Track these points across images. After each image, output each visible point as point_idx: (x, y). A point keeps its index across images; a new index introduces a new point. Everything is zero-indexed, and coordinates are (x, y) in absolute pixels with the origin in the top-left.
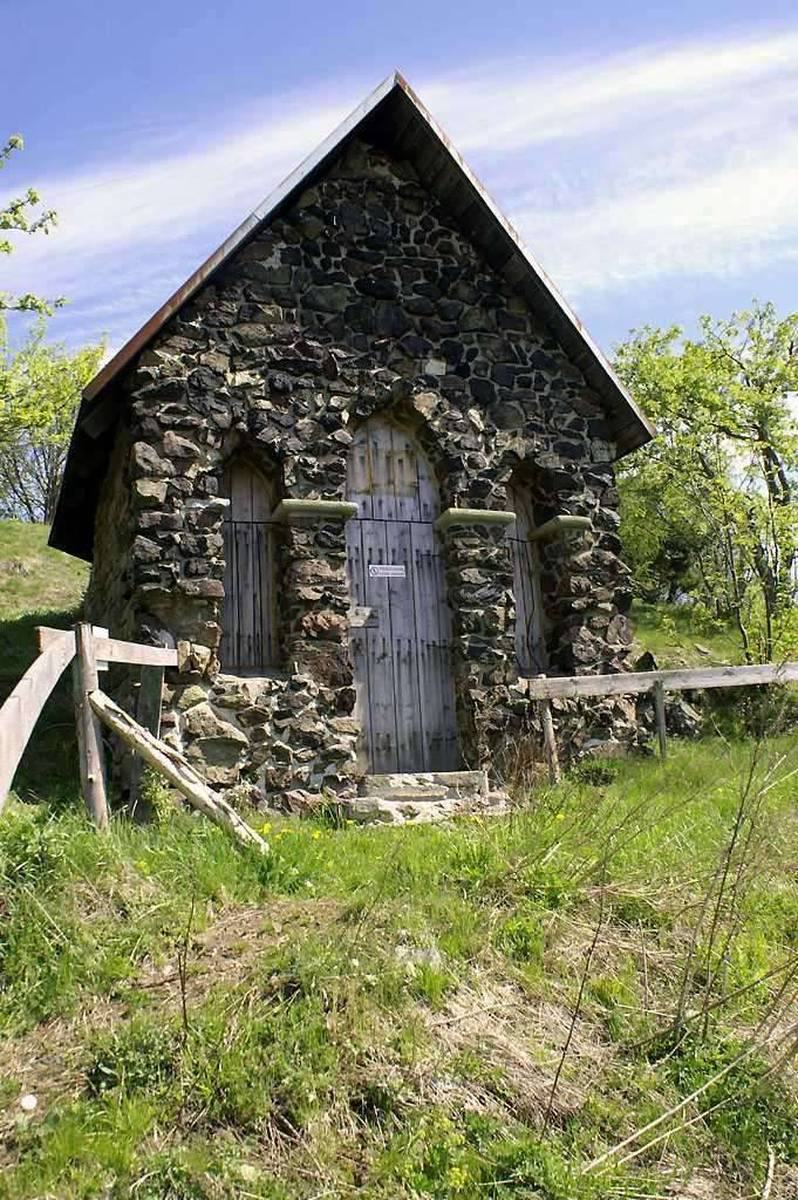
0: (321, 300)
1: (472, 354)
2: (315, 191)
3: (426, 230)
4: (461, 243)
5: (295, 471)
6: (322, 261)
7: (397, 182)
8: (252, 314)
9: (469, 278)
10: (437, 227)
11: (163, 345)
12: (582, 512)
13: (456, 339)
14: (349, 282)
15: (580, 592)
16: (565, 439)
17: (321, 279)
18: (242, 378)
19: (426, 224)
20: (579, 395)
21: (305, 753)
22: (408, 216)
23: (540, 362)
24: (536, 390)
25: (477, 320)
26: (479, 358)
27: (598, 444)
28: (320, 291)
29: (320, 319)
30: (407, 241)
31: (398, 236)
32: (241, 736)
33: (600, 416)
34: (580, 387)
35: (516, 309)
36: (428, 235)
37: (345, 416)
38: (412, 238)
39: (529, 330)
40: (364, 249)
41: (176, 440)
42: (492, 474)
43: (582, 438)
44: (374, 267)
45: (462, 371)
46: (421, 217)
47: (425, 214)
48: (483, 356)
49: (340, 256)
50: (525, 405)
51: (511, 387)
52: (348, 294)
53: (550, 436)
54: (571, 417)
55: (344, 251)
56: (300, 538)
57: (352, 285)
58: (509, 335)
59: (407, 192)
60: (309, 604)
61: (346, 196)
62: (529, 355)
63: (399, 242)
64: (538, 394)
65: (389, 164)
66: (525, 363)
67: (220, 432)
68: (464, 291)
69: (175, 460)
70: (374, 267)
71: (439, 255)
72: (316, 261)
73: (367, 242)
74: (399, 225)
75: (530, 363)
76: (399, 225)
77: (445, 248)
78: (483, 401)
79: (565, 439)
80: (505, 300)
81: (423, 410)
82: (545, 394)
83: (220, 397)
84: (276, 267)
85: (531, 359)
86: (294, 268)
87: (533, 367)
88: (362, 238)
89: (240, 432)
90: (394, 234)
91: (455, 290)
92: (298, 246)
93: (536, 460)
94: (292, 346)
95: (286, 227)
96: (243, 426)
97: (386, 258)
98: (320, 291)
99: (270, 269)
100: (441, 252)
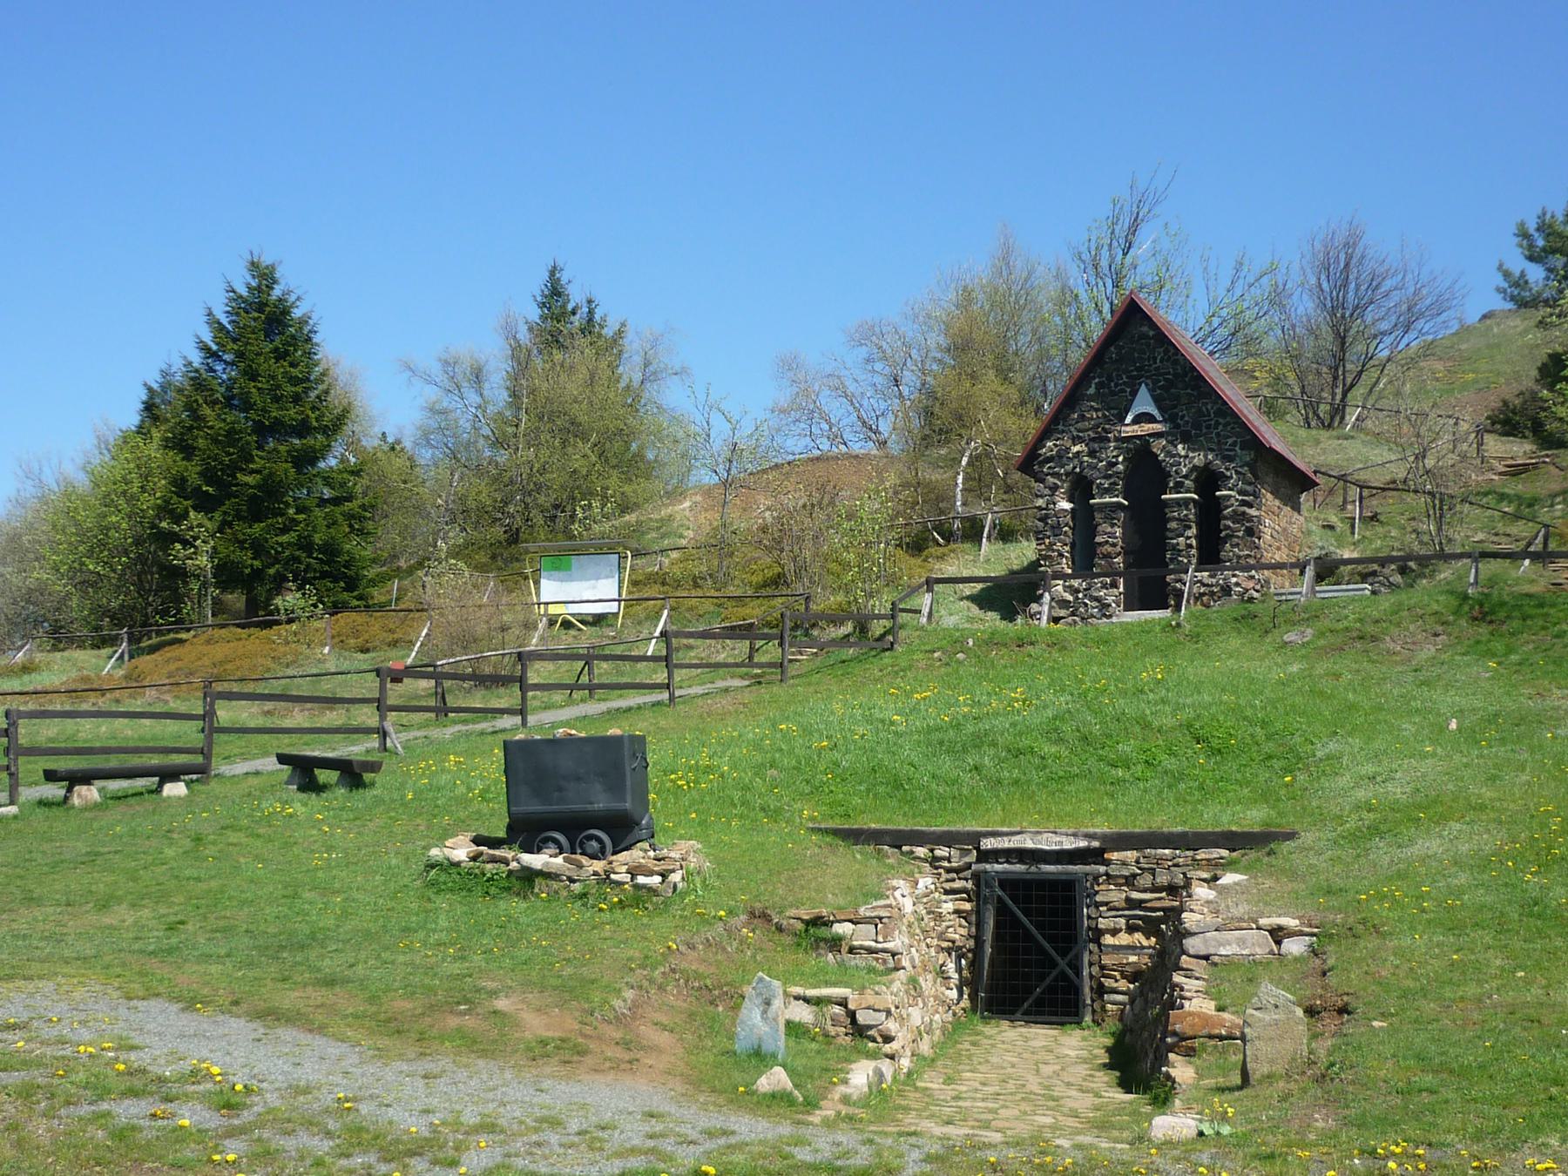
1: (1183, 416)
2: (1112, 349)
5: (1098, 487)
7: (1151, 333)
8: (1082, 418)
11: (1049, 439)
12: (1230, 489)
15: (1228, 527)
17: (1113, 393)
18: (1076, 449)
21: (1095, 604)
32: (1071, 598)
37: (1121, 459)
41: (1050, 479)
42: (1186, 477)
45: (1177, 426)
54: (1230, 441)
56: (1098, 516)
60: (1100, 544)
67: (1067, 474)
69: (1050, 489)
73: (1137, 369)
78: (1186, 439)
96: (1078, 470)
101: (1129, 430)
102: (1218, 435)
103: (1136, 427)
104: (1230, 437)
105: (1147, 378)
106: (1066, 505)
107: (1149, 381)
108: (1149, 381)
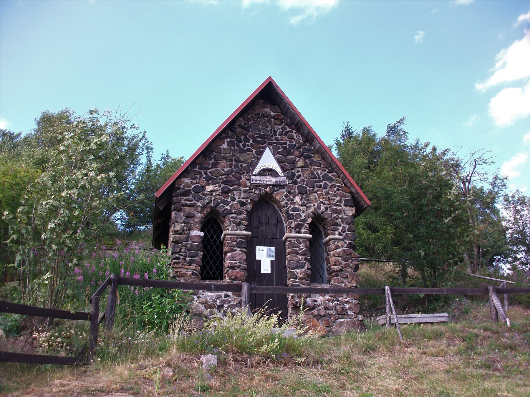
0: (242, 159)
1: (300, 176)
2: (241, 119)
3: (283, 131)
4: (297, 135)
6: (243, 145)
7: (272, 114)
9: (300, 147)
10: (288, 129)
11: (185, 177)
13: (293, 171)
14: (252, 151)
16: (334, 207)
17: (242, 151)
19: (283, 129)
20: (341, 190)
22: (276, 126)
23: (326, 178)
24: (324, 188)
25: (300, 163)
26: (302, 178)
27: (348, 208)
28: (242, 156)
29: (241, 166)
30: (276, 135)
31: (272, 133)
33: (350, 198)
34: (342, 187)
35: (316, 158)
36: (284, 133)
37: (249, 201)
38: (277, 134)
39: (322, 166)
40: (259, 139)
42: (304, 221)
43: (341, 206)
44: (262, 146)
46: (281, 126)
47: (283, 124)
48: (303, 176)
49: (250, 142)
50: (319, 194)
51: (314, 188)
52: (253, 156)
53: (328, 206)
54: (338, 198)
55: (251, 140)
57: (254, 153)
58: (314, 168)
59: (276, 117)
61: (253, 120)
62: (322, 175)
63: (272, 136)
64: (324, 190)
65: (269, 107)
66: (320, 179)
68: (297, 153)
70: (262, 146)
71: (288, 139)
72: (241, 145)
74: (273, 129)
75: (322, 178)
76: (273, 129)
77: (290, 137)
79: (334, 207)
80: (313, 155)
81: (278, 198)
82: (327, 190)
83: (205, 195)
84: (225, 148)
85: (322, 177)
86: (232, 148)
87: (323, 180)
88: (258, 135)
89: (211, 207)
90: (271, 133)
91: (293, 153)
92: (234, 139)
93: (322, 215)
94: (231, 176)
95: (230, 133)
97: (268, 142)
98: (242, 156)
99: (223, 148)
100: (289, 138)
101: (257, 180)
102: (327, 193)
103: (263, 178)
104: (335, 196)
105: (269, 144)
106: (197, 233)
107: (271, 147)
108: (271, 147)
